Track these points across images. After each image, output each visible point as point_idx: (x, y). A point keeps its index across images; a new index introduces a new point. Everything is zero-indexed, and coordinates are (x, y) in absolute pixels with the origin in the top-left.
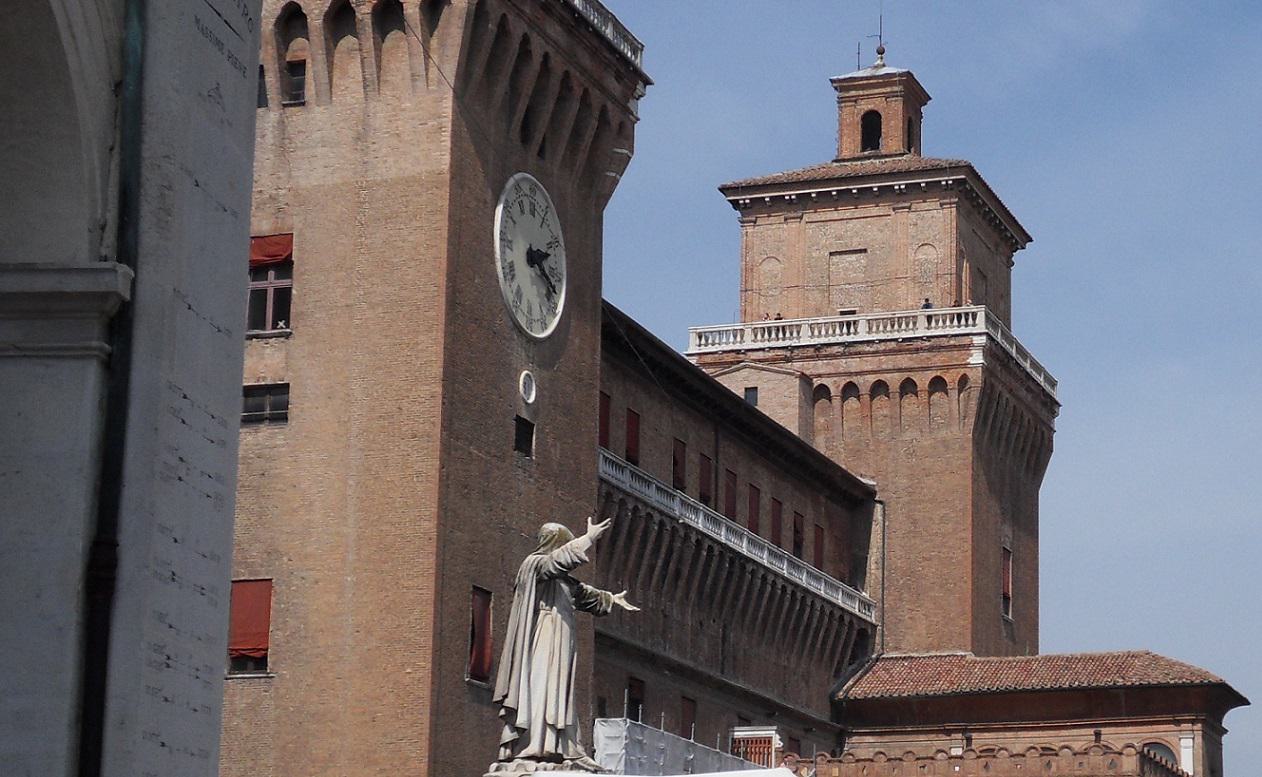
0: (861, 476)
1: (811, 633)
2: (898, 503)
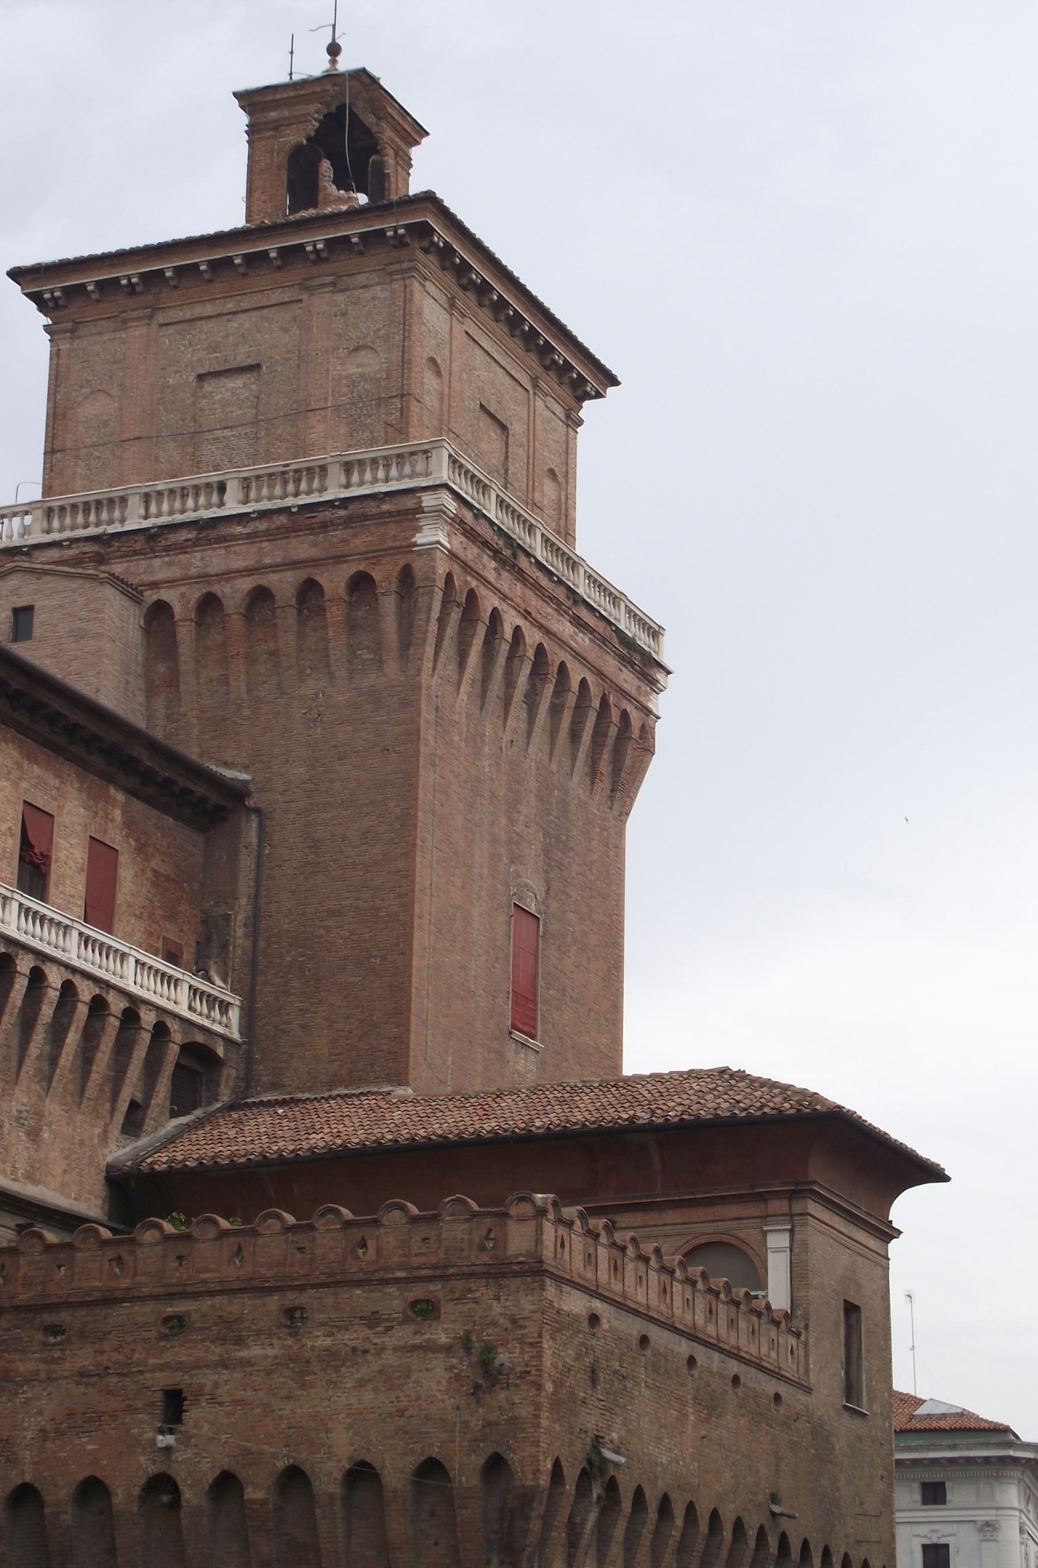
0: (226, 764)
1: (39, 1036)
2: (286, 812)
